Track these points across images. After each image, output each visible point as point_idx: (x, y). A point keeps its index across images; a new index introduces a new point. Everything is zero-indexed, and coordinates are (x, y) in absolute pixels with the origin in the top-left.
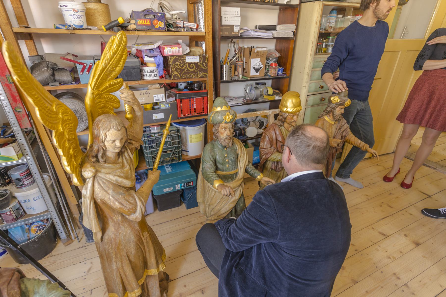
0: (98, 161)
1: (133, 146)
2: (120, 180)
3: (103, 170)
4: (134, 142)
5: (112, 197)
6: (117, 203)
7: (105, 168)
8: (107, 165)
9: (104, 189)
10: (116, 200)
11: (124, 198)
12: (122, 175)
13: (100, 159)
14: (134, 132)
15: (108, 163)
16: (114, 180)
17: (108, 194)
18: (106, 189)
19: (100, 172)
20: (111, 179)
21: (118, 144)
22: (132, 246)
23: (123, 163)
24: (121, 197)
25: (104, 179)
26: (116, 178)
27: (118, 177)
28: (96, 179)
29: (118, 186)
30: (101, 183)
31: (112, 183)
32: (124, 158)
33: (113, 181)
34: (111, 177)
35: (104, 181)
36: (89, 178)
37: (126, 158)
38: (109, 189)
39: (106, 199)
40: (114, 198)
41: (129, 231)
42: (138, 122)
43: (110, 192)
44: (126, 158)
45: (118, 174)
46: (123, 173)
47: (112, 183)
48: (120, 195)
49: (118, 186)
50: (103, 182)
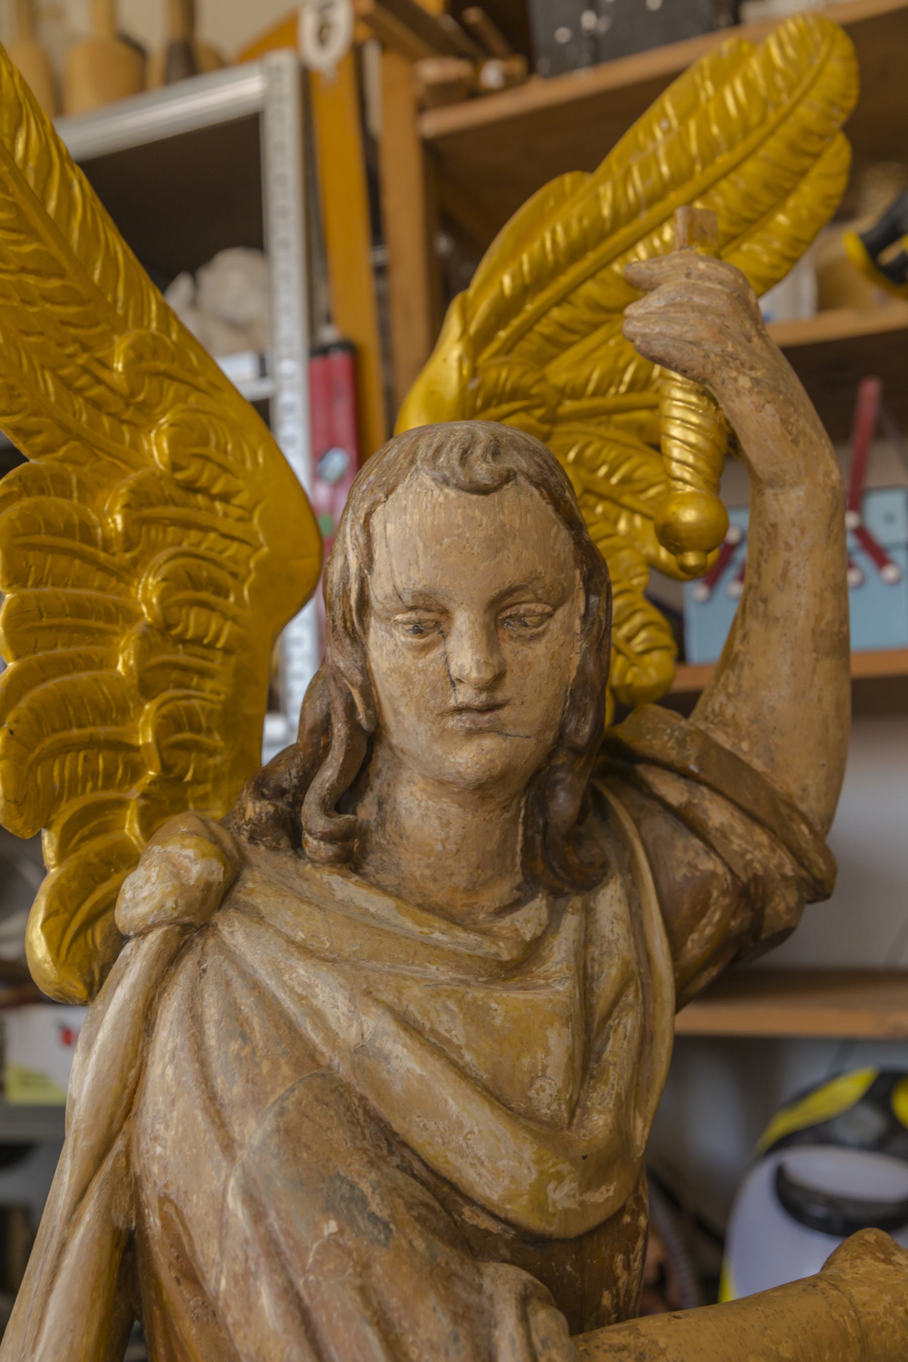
0: (288, 829)
1: (708, 864)
2: (404, 1061)
3: (289, 917)
4: (717, 814)
5: (251, 1199)
6: (266, 1299)
7: (319, 903)
8: (345, 888)
9: (205, 1080)
10: (272, 1250)
11: (365, 1267)
12: (452, 1027)
13: (314, 818)
14: (745, 713)
16: (350, 1035)
17: (228, 1146)
18: (231, 1088)
19: (257, 917)
20: (317, 1016)
21: (464, 654)
23: (531, 952)
24: (333, 1242)
25: (256, 987)
26: (375, 1024)
27: (389, 1025)
28: (188, 965)
29: (354, 1129)
30: (212, 1011)
31: (306, 1059)
32: (570, 923)
33: (331, 1037)
34: (330, 996)
35: (247, 1003)
36: (142, 934)
37: (586, 939)
38: (256, 1100)
39: (197, 1207)
40: (258, 1216)
42: (779, 604)
43: (254, 1131)
44: (586, 939)
45: (415, 1001)
46: (476, 1015)
48: (329, 1209)
49: (354, 1129)
50: (232, 1011)
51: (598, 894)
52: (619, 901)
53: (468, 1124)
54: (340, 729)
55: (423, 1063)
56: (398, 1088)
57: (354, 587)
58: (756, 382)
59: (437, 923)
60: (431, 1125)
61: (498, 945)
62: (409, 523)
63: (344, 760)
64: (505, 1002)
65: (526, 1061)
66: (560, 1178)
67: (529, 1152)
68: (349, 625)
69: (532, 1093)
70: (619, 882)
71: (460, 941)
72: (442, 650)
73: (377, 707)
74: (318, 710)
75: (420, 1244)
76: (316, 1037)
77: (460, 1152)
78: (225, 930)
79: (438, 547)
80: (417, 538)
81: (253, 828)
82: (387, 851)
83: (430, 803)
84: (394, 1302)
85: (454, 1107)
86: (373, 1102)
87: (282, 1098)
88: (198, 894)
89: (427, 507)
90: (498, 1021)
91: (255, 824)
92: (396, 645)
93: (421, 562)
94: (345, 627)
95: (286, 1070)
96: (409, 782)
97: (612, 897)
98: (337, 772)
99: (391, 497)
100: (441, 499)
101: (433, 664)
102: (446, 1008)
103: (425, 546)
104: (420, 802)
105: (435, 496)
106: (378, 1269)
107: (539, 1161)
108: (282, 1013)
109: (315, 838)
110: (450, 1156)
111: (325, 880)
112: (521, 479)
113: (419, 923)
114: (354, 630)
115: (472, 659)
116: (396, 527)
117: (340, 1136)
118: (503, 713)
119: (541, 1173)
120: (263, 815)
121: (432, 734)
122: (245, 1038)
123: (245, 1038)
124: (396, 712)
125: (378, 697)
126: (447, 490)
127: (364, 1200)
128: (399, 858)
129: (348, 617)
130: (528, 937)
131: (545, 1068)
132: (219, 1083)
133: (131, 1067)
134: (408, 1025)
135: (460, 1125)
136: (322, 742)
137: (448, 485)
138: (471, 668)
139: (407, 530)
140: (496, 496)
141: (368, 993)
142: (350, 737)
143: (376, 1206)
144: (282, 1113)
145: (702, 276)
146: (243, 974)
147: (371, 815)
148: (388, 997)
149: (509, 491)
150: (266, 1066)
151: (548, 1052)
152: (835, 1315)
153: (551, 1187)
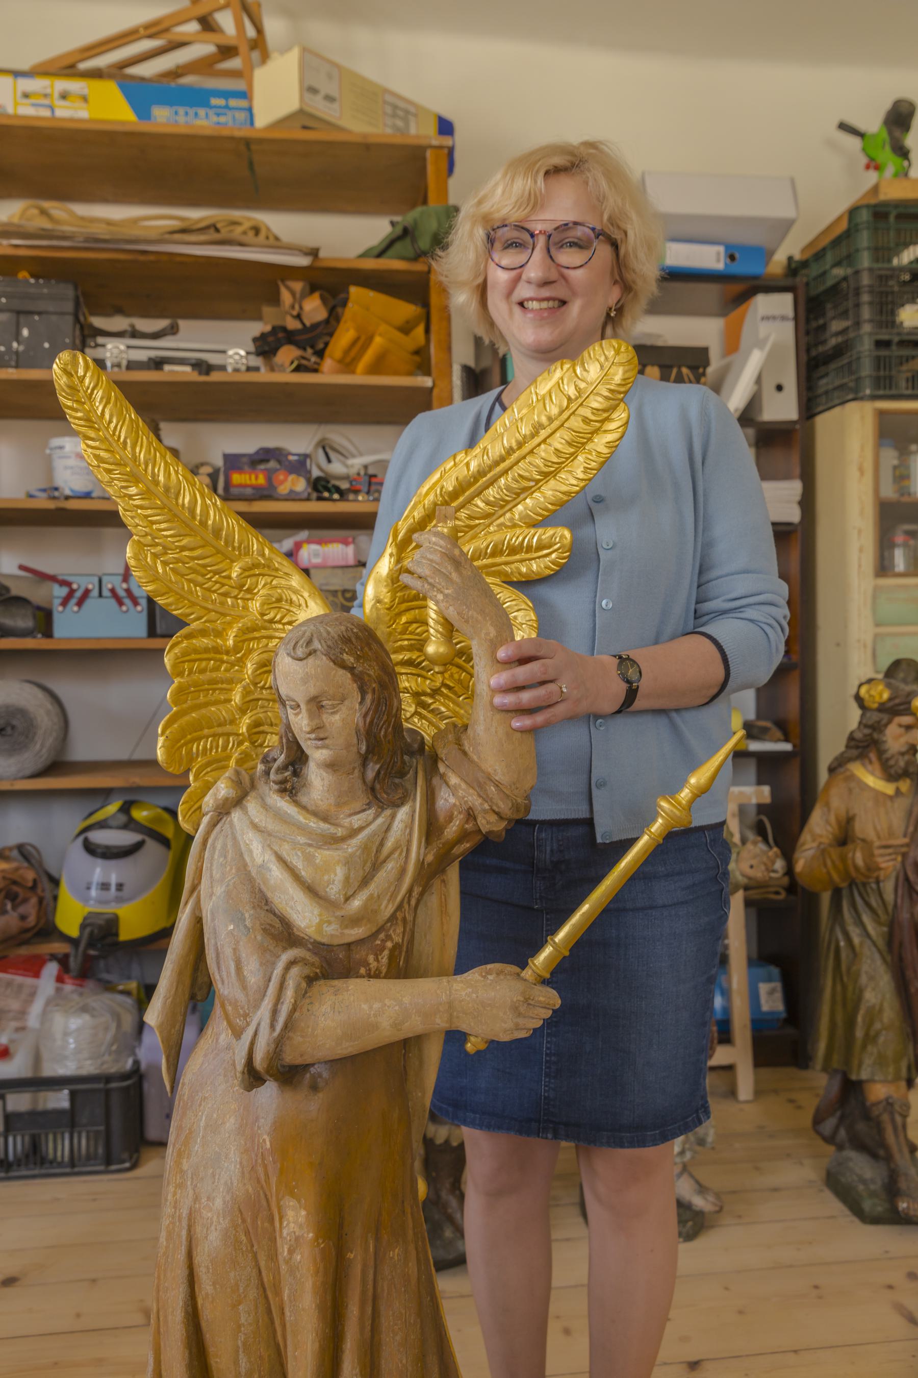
2: (276, 873)
12: (298, 863)
15: (297, 803)
20: (251, 851)
22: (218, 1203)
24: (231, 932)
25: (234, 838)
26: (269, 857)
27: (273, 858)
33: (253, 860)
35: (230, 843)
41: (231, 1123)
45: (285, 850)
46: (309, 859)
47: (245, 865)
48: (232, 921)
50: (225, 846)
53: (296, 898)
55: (282, 874)
56: (272, 882)
58: (446, 596)
59: (313, 819)
60: (282, 897)
64: (322, 855)
65: (326, 878)
66: (329, 923)
67: (316, 911)
69: (328, 890)
75: (259, 938)
76: (248, 859)
77: (292, 908)
78: (233, 815)
84: (244, 955)
85: (291, 891)
86: (262, 886)
87: (230, 880)
88: (221, 802)
90: (317, 861)
95: (234, 871)
102: (297, 854)
106: (241, 943)
107: (320, 915)
108: (240, 850)
110: (288, 909)
112: (318, 653)
113: (306, 819)
117: (246, 897)
118: (327, 742)
119: (321, 920)
122: (225, 857)
123: (225, 857)
127: (244, 920)
130: (356, 827)
131: (334, 881)
132: (214, 872)
133: (199, 861)
134: (281, 859)
135: (293, 898)
140: (305, 661)
141: (269, 846)
142: (287, 743)
143: (248, 923)
144: (227, 886)
145: (434, 543)
146: (233, 833)
148: (276, 848)
149: (311, 660)
150: (228, 868)
151: (336, 875)
152: (438, 992)
153: (325, 925)
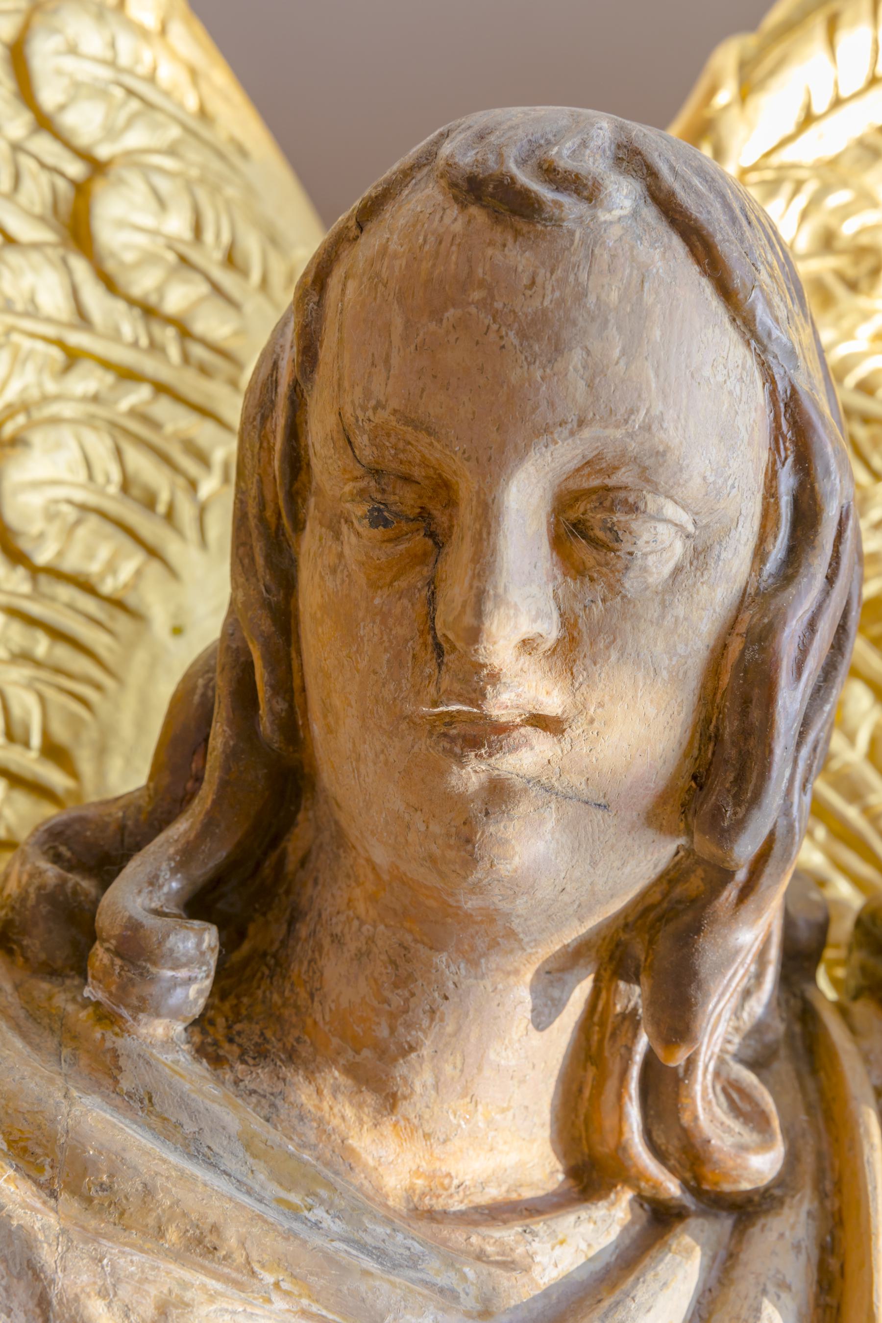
51: (753, 1225)
52: (797, 1247)
54: (220, 736)
57: (280, 419)
61: (459, 1271)
62: (385, 274)
63: (214, 802)
68: (269, 513)
70: (806, 1206)
71: (369, 1239)
72: (426, 571)
73: (298, 699)
74: (196, 698)
79: (433, 326)
80: (396, 306)
81: (10, 915)
82: (279, 1019)
83: (381, 928)
89: (425, 241)
91: (13, 908)
92: (341, 555)
93: (395, 360)
94: (261, 519)
96: (348, 876)
97: (782, 1236)
98: (198, 826)
99: (370, 226)
100: (458, 227)
101: (405, 601)
103: (408, 324)
104: (362, 923)
105: (447, 220)
109: (108, 950)
111: (108, 1044)
114: (279, 526)
115: (471, 587)
116: (361, 283)
120: (32, 890)
121: (386, 762)
124: (327, 709)
125: (302, 677)
126: (474, 210)
128: (298, 1040)
129: (269, 496)
136: (194, 766)
137: (478, 199)
138: (464, 606)
139: (381, 287)
147: (272, 942)
